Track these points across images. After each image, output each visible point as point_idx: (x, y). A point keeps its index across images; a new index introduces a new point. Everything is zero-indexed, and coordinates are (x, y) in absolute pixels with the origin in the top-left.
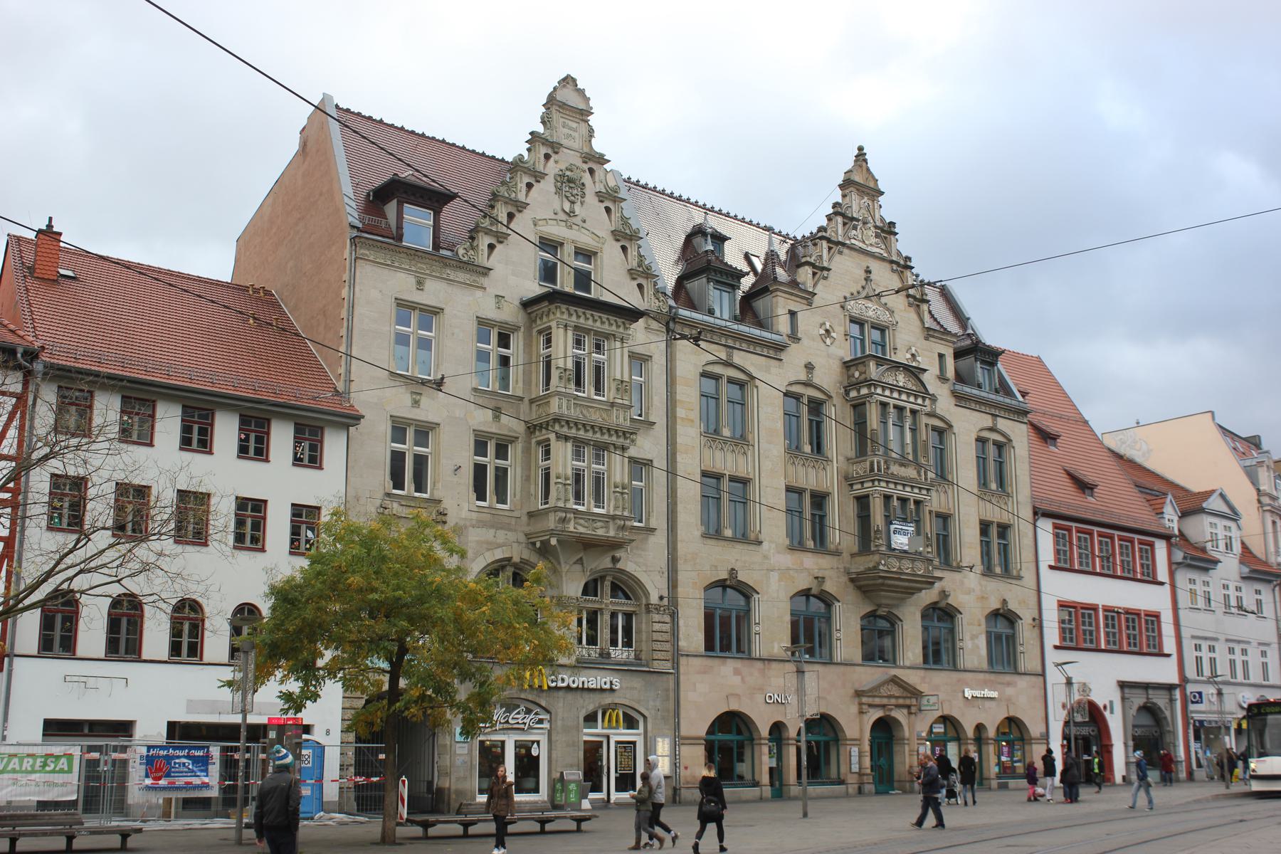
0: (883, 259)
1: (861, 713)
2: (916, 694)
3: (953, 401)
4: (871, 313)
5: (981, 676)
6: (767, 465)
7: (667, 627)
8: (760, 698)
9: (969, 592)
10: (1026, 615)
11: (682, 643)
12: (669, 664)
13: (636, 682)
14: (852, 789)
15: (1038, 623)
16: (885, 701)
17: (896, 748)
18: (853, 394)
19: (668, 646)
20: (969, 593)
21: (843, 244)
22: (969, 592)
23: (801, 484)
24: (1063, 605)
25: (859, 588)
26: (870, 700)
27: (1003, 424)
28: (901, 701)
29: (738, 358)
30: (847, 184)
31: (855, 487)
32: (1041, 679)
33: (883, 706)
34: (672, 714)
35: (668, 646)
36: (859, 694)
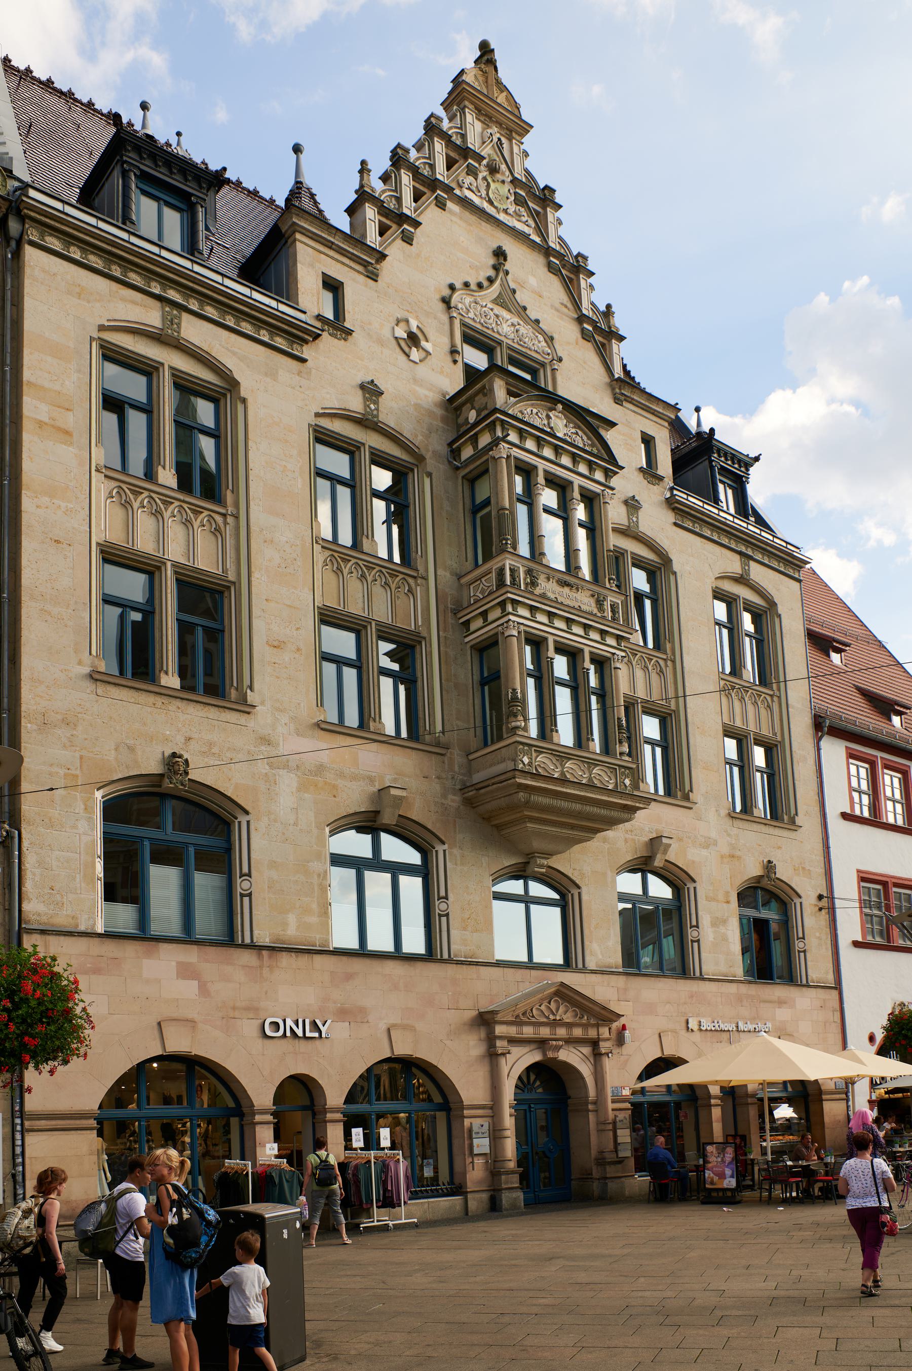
0: (533, 245)
1: (493, 1056)
2: (603, 1015)
3: (670, 517)
4: (506, 329)
5: (732, 988)
6: (265, 558)
8: (250, 1028)
9: (708, 843)
10: (808, 889)
14: (477, 1201)
15: (827, 902)
16: (545, 1032)
17: (574, 1122)
18: (467, 452)
20: (706, 846)
21: (449, 189)
22: (708, 843)
23: (356, 608)
24: (864, 878)
25: (487, 818)
26: (512, 1031)
27: (757, 573)
28: (578, 1032)
29: (193, 330)
30: (459, 95)
31: (473, 627)
32: (835, 993)
33: (541, 1043)
36: (485, 1021)
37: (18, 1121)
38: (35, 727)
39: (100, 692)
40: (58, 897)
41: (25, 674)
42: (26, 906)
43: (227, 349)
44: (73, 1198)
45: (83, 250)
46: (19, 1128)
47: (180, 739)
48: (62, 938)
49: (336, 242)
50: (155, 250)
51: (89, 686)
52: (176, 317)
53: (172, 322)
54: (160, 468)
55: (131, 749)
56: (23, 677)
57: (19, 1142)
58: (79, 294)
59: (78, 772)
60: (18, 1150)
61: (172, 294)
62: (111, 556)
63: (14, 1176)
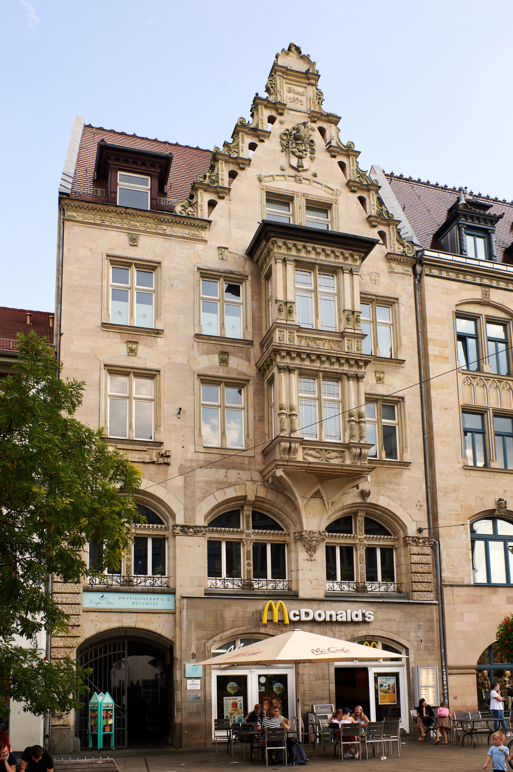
7: (429, 559)
11: (446, 575)
12: (432, 595)
13: (395, 614)
19: (430, 578)
34: (437, 644)
35: (430, 578)
37: (444, 670)
38: (442, 494)
39: (467, 474)
40: (456, 570)
41: (437, 471)
42: (443, 575)
43: (510, 300)
44: (468, 705)
45: (447, 272)
46: (445, 673)
47: (502, 492)
48: (459, 588)
50: (476, 262)
51: (463, 472)
52: (487, 291)
53: (486, 294)
54: (484, 364)
55: (482, 499)
56: (436, 472)
57: (445, 679)
58: (447, 292)
59: (460, 512)
60: (445, 683)
61: (486, 281)
62: (466, 410)
63: (443, 694)
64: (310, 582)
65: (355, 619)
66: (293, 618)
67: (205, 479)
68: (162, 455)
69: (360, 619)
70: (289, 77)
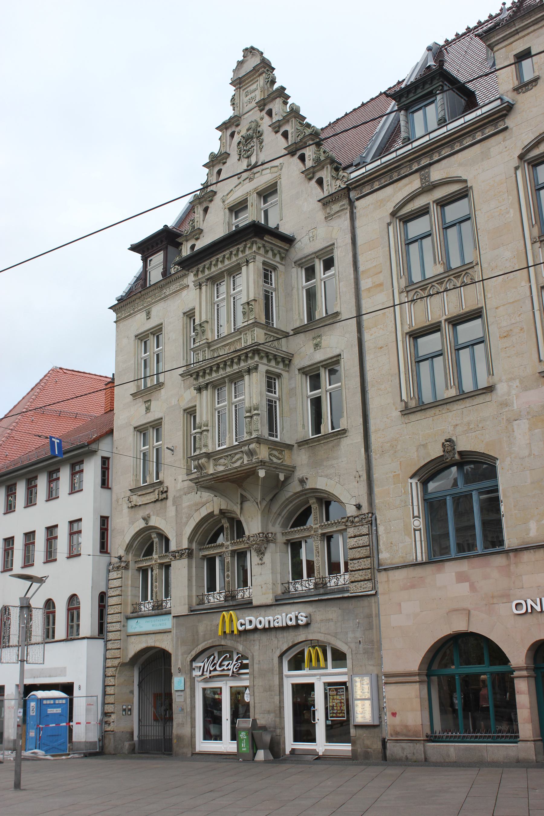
49: (517, 28)
64: (260, 587)
65: (290, 623)
66: (241, 628)
67: (188, 503)
68: (162, 492)
69: (293, 623)
70: (247, 81)
